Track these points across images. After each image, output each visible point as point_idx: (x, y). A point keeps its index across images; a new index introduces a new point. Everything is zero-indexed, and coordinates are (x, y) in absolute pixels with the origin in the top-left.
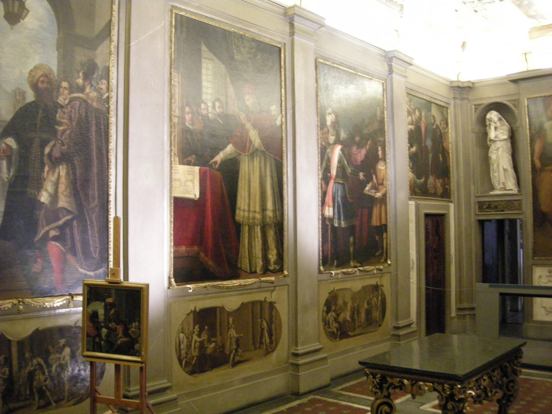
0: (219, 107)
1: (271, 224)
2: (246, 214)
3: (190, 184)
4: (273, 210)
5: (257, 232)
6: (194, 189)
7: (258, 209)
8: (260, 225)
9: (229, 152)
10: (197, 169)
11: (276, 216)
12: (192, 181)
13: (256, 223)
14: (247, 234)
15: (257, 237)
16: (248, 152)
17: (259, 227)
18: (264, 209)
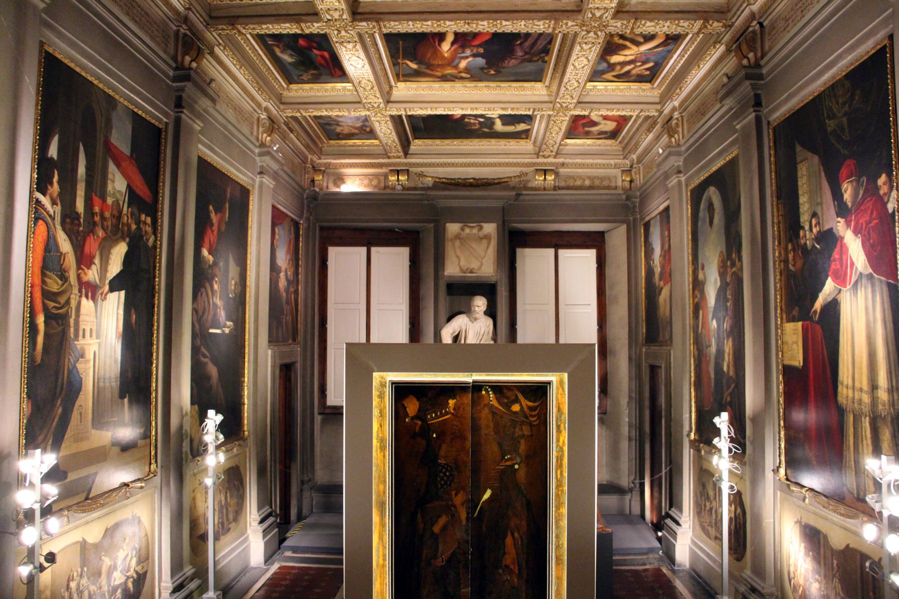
0: (816, 226)
1: (885, 416)
2: (850, 392)
3: (795, 346)
4: (888, 389)
5: (865, 428)
6: (798, 353)
7: (865, 386)
8: (870, 415)
9: (827, 293)
10: (800, 324)
11: (893, 400)
12: (796, 343)
13: (864, 411)
14: (851, 430)
15: (866, 436)
16: (850, 284)
17: (867, 419)
18: (874, 387)
